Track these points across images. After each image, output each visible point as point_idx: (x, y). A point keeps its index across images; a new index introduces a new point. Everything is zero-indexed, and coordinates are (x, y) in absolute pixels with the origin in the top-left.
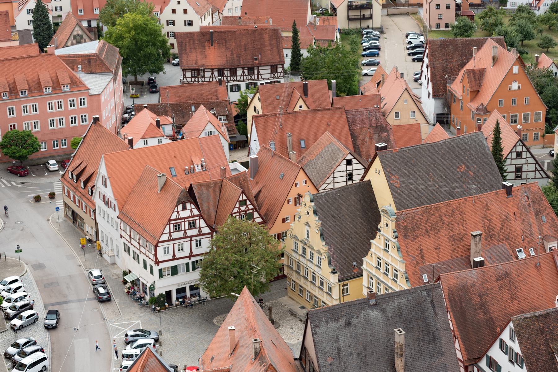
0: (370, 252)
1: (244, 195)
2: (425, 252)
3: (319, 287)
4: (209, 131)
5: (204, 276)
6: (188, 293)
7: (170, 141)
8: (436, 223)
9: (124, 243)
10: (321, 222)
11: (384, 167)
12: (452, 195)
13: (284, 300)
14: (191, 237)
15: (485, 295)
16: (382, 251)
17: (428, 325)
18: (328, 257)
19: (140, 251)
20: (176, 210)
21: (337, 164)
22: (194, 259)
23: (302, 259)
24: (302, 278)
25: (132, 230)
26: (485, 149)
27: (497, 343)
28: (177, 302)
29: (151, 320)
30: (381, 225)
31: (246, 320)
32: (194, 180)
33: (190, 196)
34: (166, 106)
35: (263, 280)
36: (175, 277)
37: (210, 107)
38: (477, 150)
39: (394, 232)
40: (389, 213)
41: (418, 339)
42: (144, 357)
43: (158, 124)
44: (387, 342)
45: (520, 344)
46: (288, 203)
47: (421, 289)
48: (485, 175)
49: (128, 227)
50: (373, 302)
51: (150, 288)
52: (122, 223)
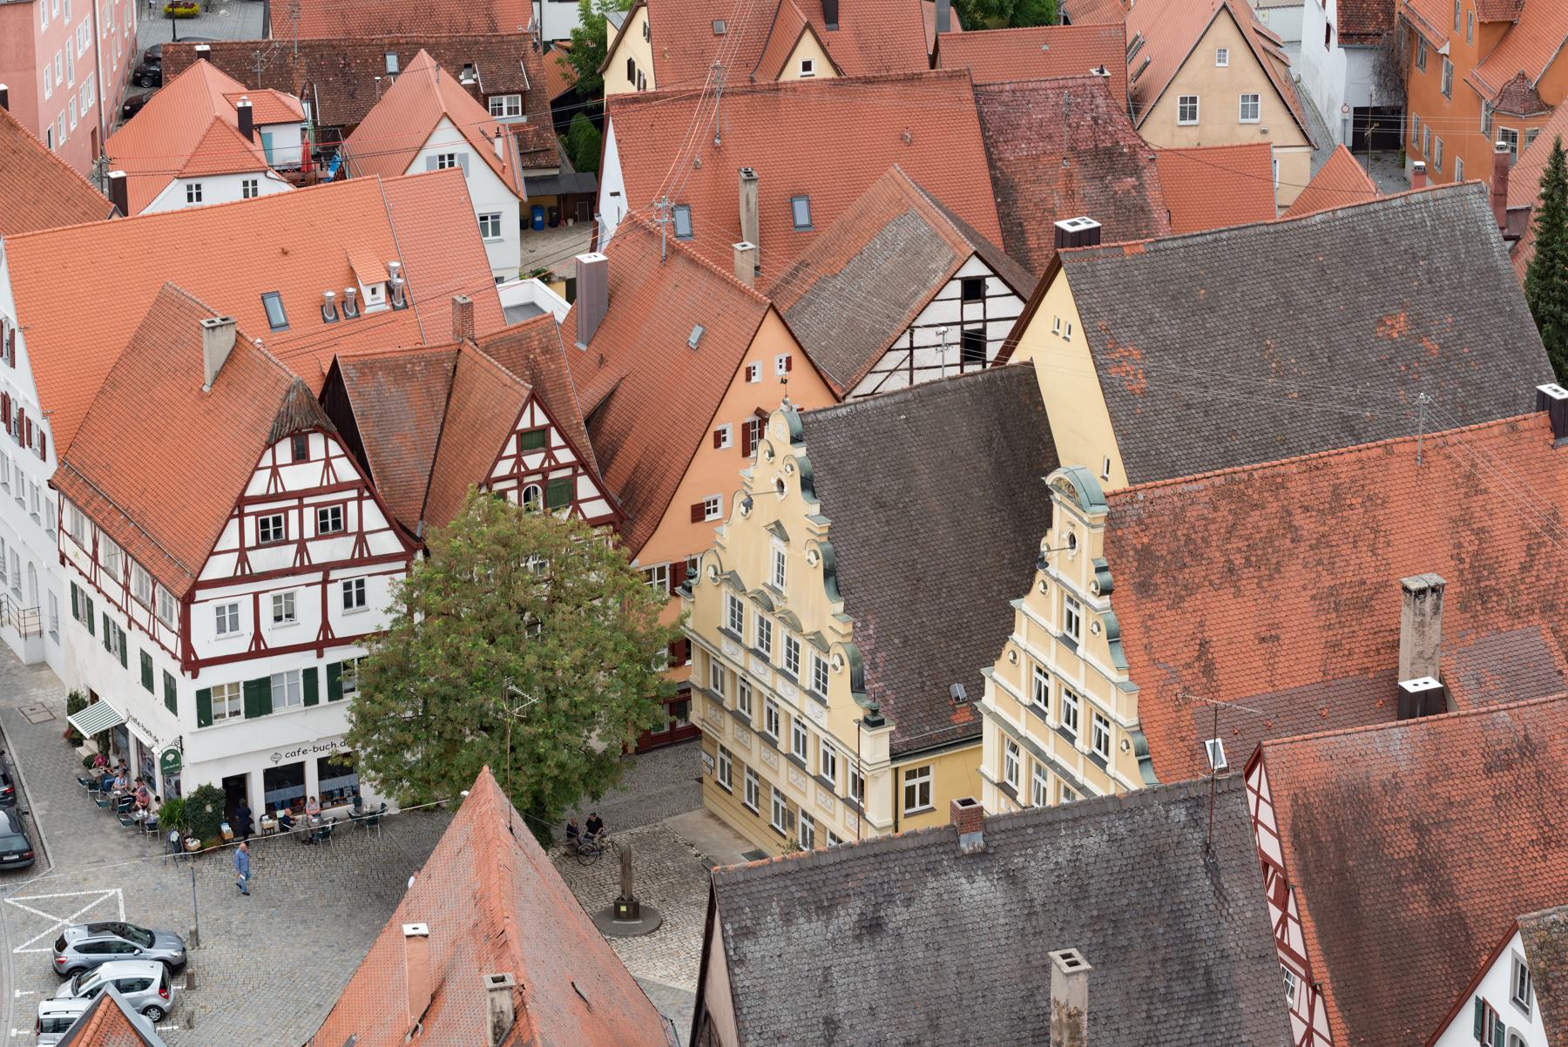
0: (1009, 646)
1: (537, 409)
2: (1217, 651)
3: (819, 780)
4: (446, 151)
5: (366, 723)
6: (313, 784)
7: (288, 188)
8: (1269, 540)
9: (74, 586)
10: (827, 522)
11: (1085, 312)
12: (1351, 431)
13: (690, 823)
14: (326, 568)
15: (1437, 824)
16: (1053, 642)
17: (1188, 938)
18: (854, 662)
19: (131, 619)
20: (267, 460)
21: (924, 294)
22: (334, 655)
23: (755, 666)
24: (755, 742)
25: (101, 537)
26: (1490, 253)
27: (1467, 1016)
28: (268, 823)
29: (165, 887)
30: (1053, 540)
31: (478, 899)
32: (349, 346)
33: (333, 409)
34: (285, 51)
35: (597, 744)
36: (263, 723)
37: (456, 58)
38: (1456, 257)
39: (1099, 570)
40: (1082, 496)
41: (1148, 994)
42: (89, 1032)
43: (247, 124)
44: (1025, 999)
45: (1550, 1021)
46: (717, 445)
47: (1165, 798)
48: (1486, 356)
49: (87, 522)
50: (971, 842)
51: (164, 761)
52: (67, 506)
